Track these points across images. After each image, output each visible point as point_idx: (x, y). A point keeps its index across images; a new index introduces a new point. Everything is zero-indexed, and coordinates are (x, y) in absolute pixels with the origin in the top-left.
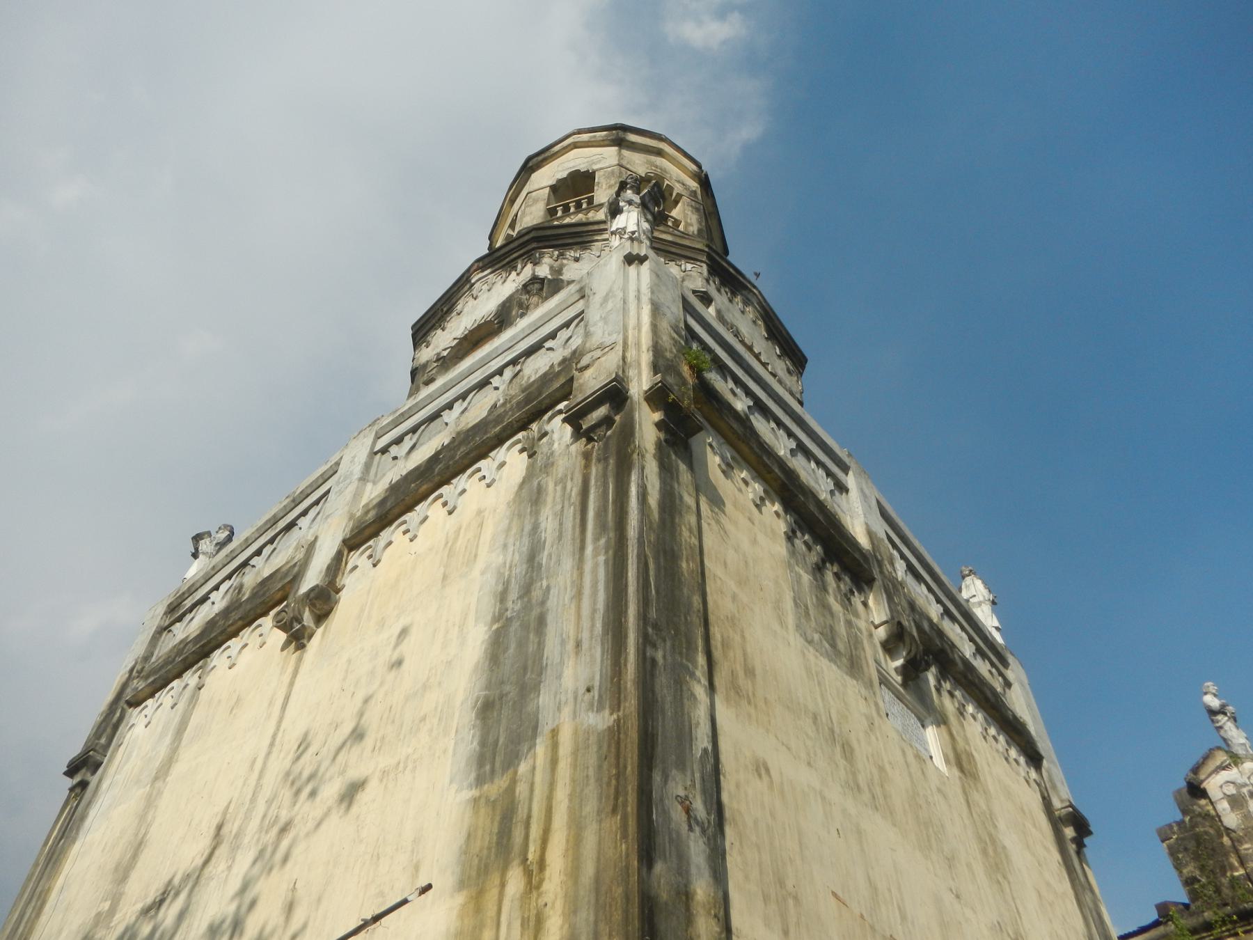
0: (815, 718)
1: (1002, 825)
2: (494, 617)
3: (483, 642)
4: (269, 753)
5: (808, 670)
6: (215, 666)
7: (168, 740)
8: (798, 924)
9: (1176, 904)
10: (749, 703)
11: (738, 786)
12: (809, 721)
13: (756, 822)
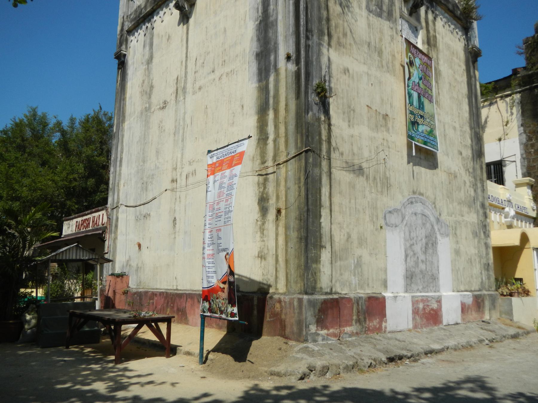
0: (369, 44)
1: (441, 62)
2: (256, 19)
3: (253, 29)
4: (186, 60)
5: (369, 25)
6: (156, 20)
7: (147, 48)
8: (353, 118)
9: (520, 68)
10: (344, 48)
11: (337, 80)
12: (366, 46)
13: (342, 90)
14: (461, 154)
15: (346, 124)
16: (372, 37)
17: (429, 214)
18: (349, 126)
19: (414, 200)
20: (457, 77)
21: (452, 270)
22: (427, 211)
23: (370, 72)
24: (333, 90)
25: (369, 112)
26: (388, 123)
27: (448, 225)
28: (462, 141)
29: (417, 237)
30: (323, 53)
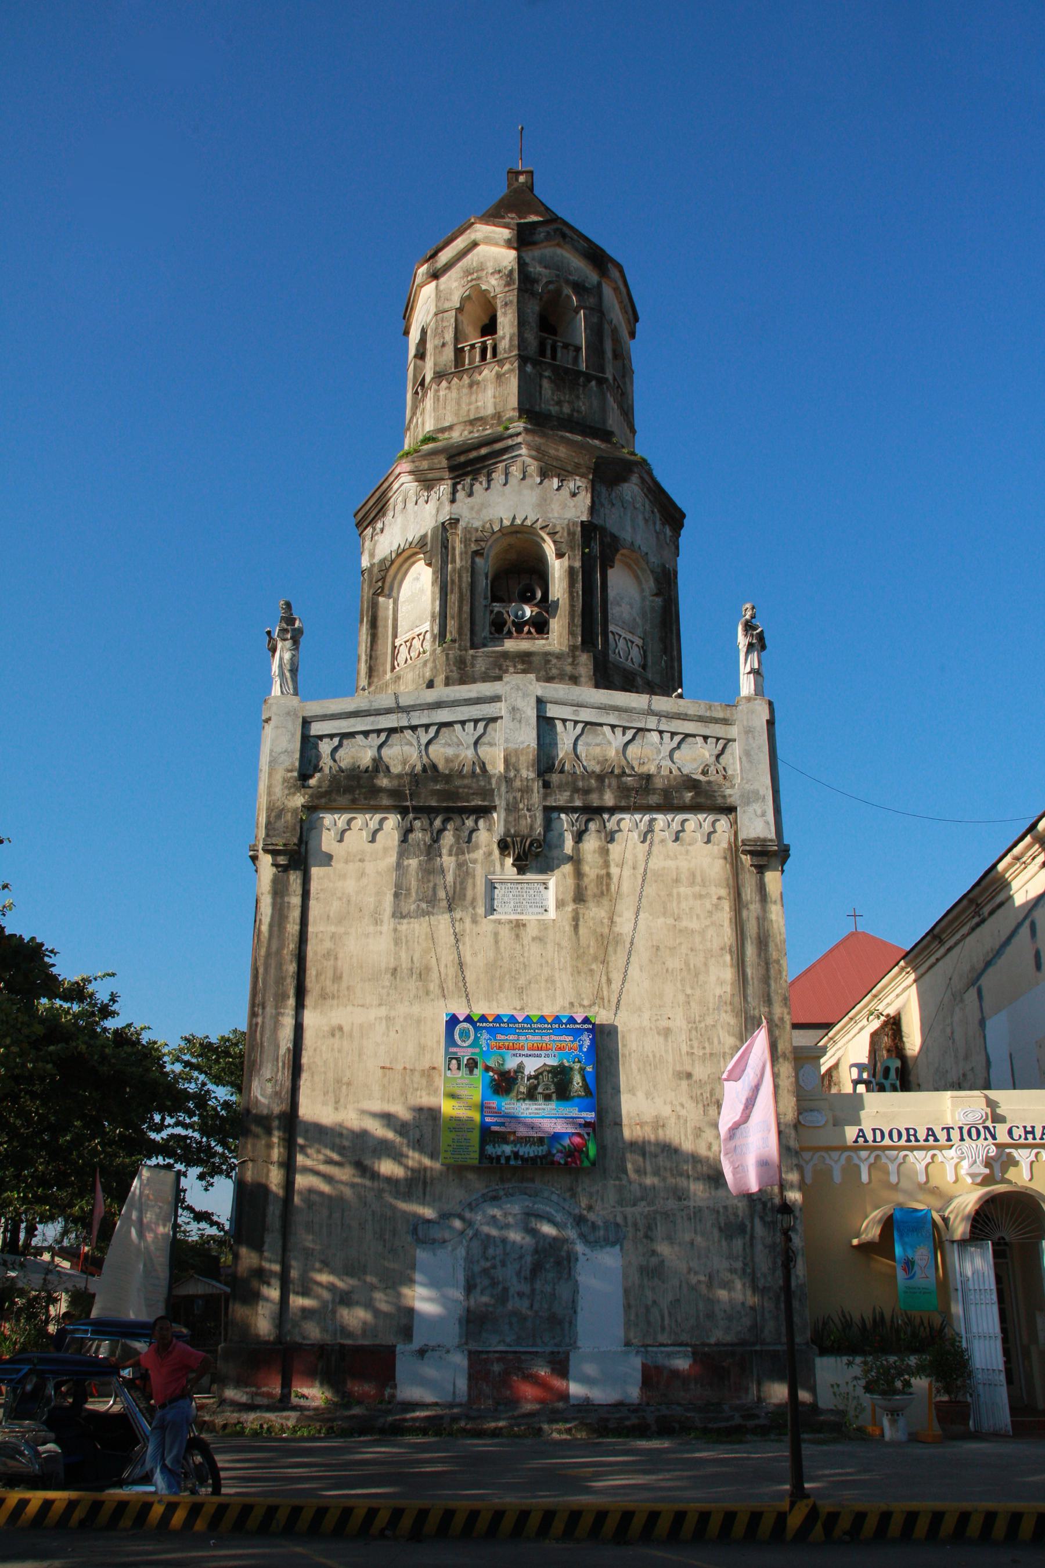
5: (397, 942)
8: (348, 1095)
10: (333, 998)
11: (315, 1050)
12: (389, 976)
14: (689, 1076)
15: (330, 1109)
16: (403, 955)
17: (548, 1209)
18: (336, 1109)
19: (501, 1193)
20: (685, 923)
21: (628, 1307)
22: (541, 1206)
23: (393, 1014)
24: (305, 1067)
25: (384, 1075)
26: (437, 1079)
27: (617, 1225)
28: (695, 1051)
29: (506, 1254)
30: (283, 1025)
